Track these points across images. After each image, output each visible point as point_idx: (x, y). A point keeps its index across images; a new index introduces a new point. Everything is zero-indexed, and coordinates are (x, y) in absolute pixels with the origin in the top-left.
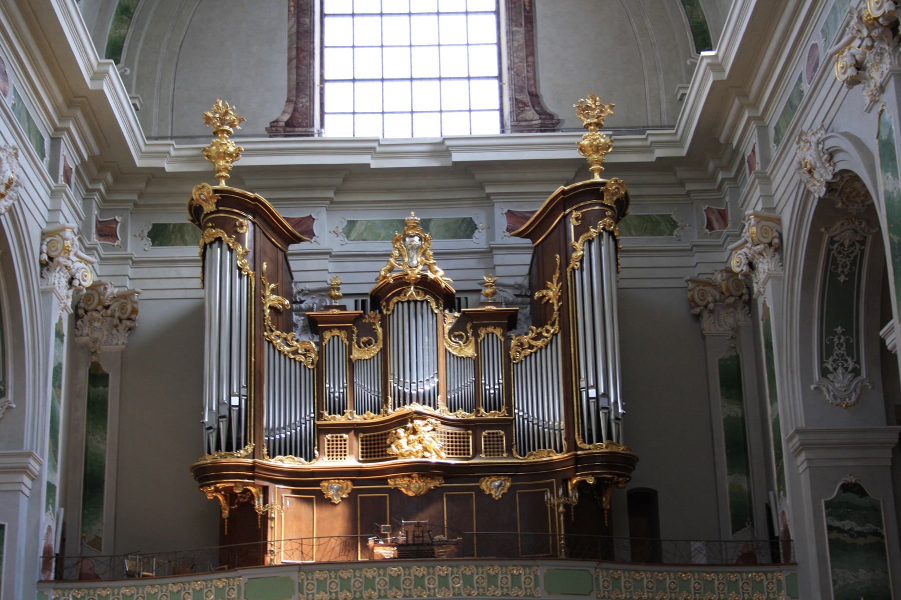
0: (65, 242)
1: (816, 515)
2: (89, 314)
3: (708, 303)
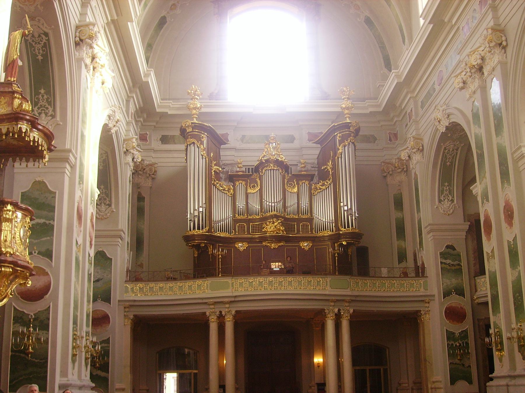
1: (436, 258)
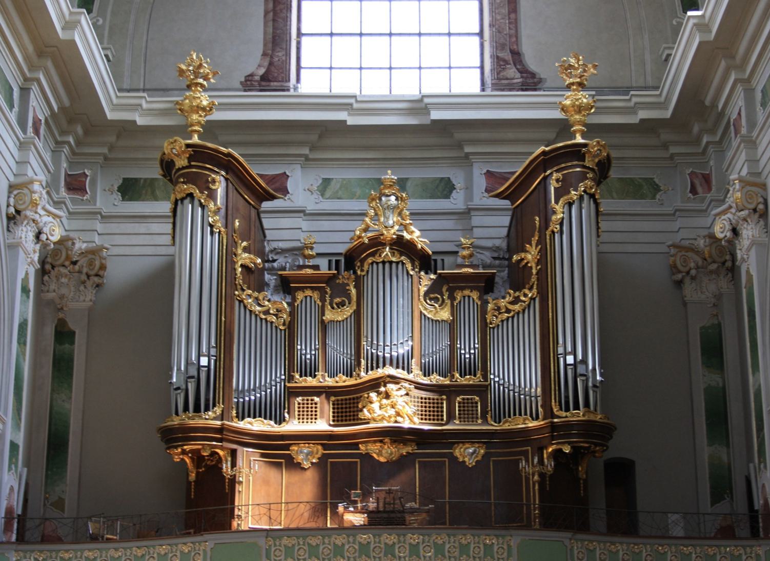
0: (33, 195)
2: (56, 269)
3: (690, 269)
